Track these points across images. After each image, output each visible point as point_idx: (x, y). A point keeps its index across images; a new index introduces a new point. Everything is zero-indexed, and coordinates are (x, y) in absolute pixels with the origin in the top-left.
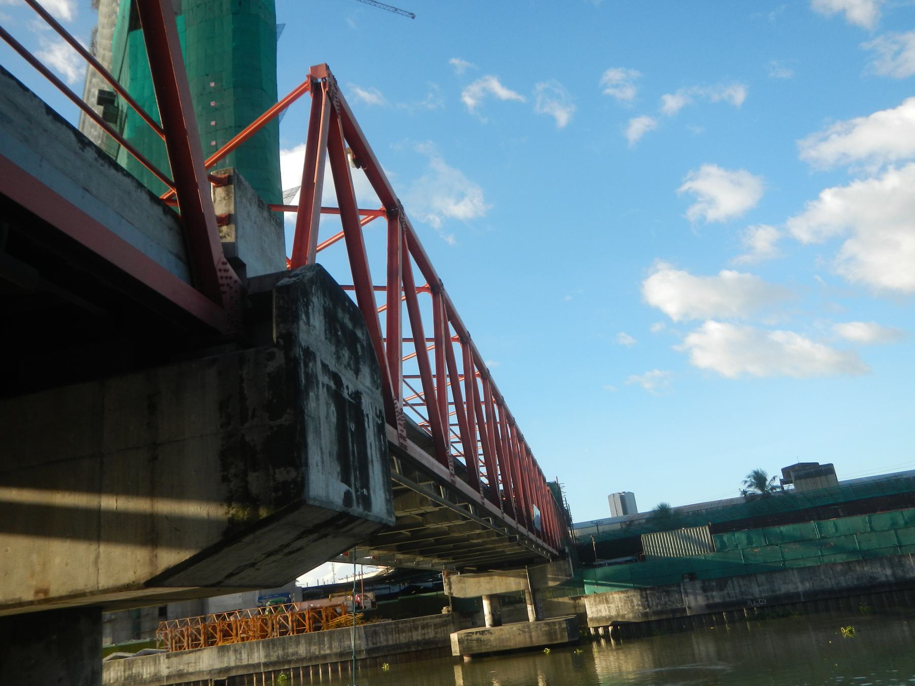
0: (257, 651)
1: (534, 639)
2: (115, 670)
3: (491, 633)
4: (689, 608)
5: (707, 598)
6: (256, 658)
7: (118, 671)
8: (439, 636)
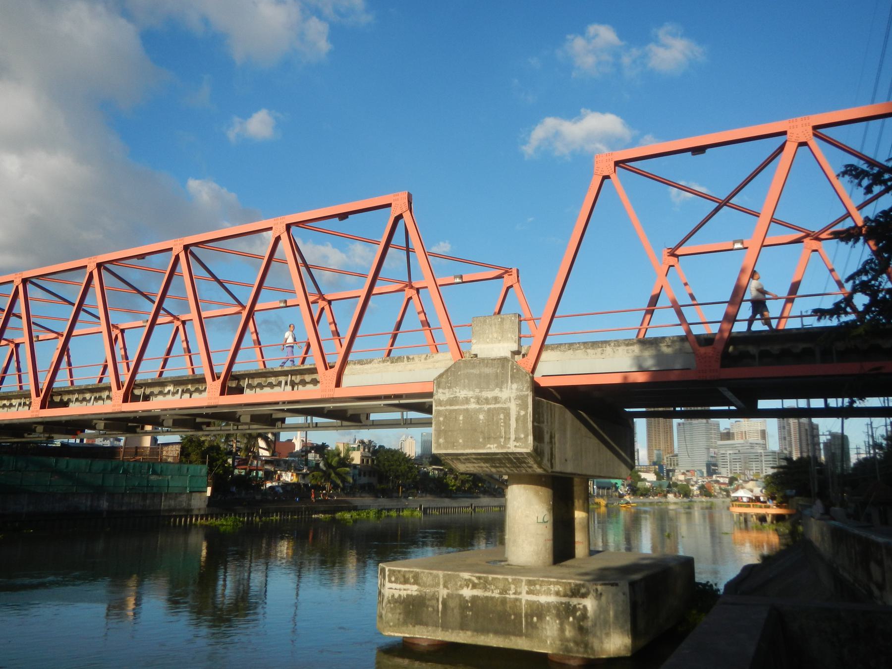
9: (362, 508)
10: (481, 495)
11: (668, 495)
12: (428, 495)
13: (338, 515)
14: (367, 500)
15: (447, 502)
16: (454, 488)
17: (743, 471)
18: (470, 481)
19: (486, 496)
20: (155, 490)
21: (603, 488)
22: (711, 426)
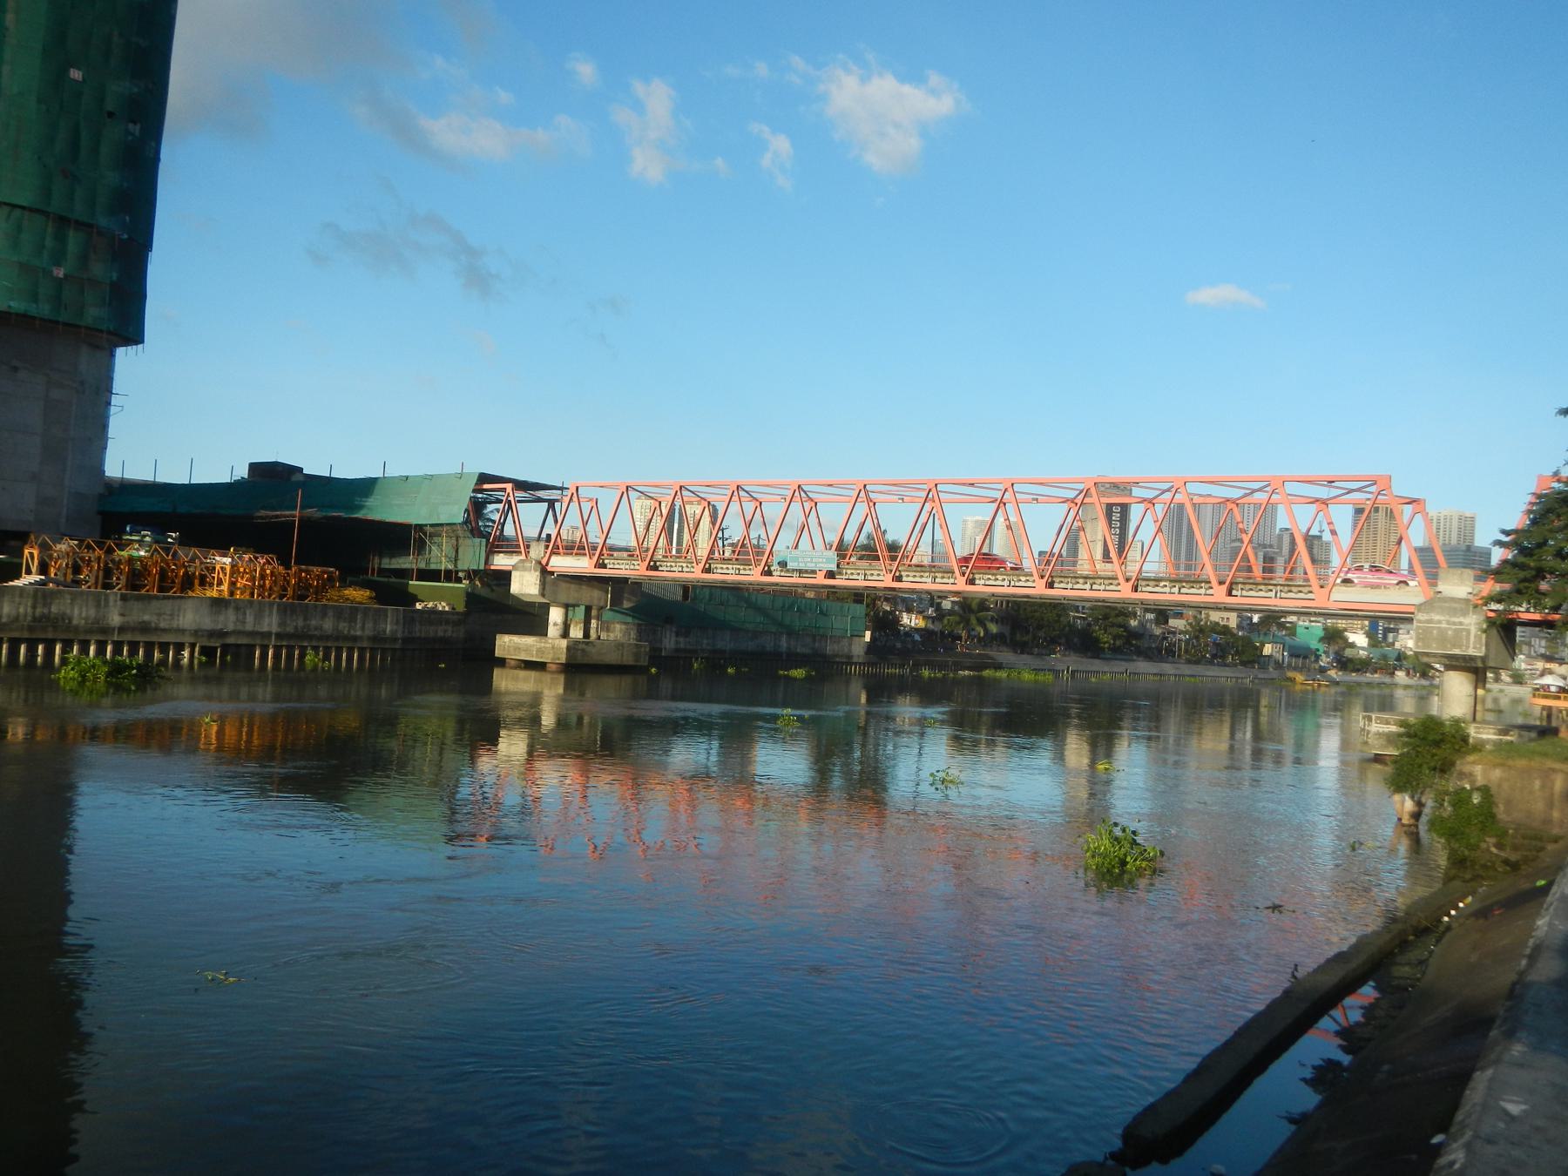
0: (269, 615)
1: (625, 658)
2: (13, 602)
3: (594, 646)
4: (665, 649)
5: (677, 642)
6: (266, 624)
7: (20, 604)
8: (455, 635)
9: (1010, 666)
10: (1135, 658)
11: (1396, 672)
12: (1072, 653)
13: (987, 673)
14: (1005, 656)
15: (1096, 665)
16: (1106, 645)
17: (1527, 640)
18: (1123, 636)
19: (1140, 659)
20: (821, 631)
21: (1298, 656)
22: (1475, 556)
